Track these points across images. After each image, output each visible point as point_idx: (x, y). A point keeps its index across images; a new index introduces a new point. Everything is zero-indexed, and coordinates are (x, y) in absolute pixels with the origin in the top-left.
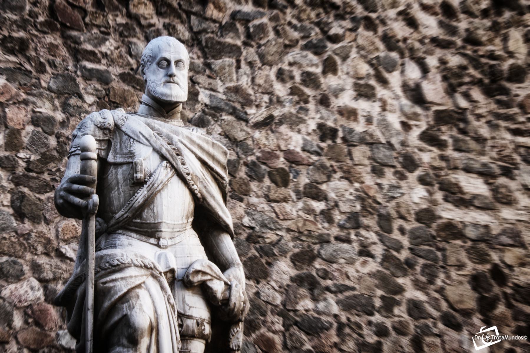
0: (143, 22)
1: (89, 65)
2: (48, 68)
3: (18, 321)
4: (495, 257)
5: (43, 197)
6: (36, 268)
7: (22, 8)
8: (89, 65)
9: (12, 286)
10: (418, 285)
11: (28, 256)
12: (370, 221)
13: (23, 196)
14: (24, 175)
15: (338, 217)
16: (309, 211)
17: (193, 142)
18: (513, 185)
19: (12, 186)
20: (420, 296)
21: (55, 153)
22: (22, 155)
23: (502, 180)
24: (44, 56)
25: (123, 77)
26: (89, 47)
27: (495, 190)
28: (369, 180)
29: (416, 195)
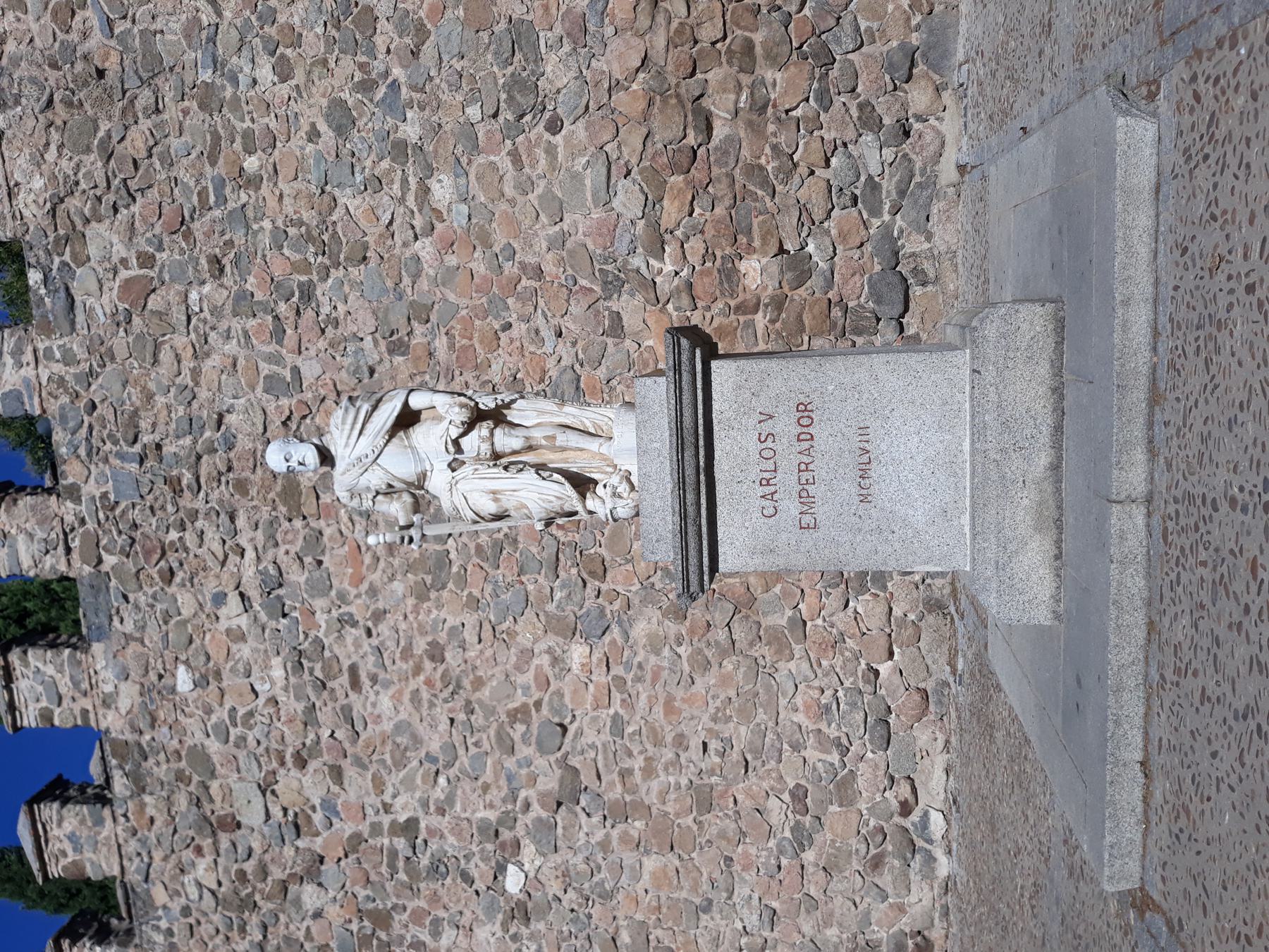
0: (151, 143)
1: (212, 199)
2: (227, 237)
3: (452, 260)
5: (344, 241)
6: (405, 245)
7: (179, 262)
8: (212, 199)
9: (425, 266)
11: (397, 251)
13: (346, 259)
14: (330, 258)
21: (303, 229)
22: (312, 261)
24: (217, 240)
25: (213, 163)
26: (195, 199)
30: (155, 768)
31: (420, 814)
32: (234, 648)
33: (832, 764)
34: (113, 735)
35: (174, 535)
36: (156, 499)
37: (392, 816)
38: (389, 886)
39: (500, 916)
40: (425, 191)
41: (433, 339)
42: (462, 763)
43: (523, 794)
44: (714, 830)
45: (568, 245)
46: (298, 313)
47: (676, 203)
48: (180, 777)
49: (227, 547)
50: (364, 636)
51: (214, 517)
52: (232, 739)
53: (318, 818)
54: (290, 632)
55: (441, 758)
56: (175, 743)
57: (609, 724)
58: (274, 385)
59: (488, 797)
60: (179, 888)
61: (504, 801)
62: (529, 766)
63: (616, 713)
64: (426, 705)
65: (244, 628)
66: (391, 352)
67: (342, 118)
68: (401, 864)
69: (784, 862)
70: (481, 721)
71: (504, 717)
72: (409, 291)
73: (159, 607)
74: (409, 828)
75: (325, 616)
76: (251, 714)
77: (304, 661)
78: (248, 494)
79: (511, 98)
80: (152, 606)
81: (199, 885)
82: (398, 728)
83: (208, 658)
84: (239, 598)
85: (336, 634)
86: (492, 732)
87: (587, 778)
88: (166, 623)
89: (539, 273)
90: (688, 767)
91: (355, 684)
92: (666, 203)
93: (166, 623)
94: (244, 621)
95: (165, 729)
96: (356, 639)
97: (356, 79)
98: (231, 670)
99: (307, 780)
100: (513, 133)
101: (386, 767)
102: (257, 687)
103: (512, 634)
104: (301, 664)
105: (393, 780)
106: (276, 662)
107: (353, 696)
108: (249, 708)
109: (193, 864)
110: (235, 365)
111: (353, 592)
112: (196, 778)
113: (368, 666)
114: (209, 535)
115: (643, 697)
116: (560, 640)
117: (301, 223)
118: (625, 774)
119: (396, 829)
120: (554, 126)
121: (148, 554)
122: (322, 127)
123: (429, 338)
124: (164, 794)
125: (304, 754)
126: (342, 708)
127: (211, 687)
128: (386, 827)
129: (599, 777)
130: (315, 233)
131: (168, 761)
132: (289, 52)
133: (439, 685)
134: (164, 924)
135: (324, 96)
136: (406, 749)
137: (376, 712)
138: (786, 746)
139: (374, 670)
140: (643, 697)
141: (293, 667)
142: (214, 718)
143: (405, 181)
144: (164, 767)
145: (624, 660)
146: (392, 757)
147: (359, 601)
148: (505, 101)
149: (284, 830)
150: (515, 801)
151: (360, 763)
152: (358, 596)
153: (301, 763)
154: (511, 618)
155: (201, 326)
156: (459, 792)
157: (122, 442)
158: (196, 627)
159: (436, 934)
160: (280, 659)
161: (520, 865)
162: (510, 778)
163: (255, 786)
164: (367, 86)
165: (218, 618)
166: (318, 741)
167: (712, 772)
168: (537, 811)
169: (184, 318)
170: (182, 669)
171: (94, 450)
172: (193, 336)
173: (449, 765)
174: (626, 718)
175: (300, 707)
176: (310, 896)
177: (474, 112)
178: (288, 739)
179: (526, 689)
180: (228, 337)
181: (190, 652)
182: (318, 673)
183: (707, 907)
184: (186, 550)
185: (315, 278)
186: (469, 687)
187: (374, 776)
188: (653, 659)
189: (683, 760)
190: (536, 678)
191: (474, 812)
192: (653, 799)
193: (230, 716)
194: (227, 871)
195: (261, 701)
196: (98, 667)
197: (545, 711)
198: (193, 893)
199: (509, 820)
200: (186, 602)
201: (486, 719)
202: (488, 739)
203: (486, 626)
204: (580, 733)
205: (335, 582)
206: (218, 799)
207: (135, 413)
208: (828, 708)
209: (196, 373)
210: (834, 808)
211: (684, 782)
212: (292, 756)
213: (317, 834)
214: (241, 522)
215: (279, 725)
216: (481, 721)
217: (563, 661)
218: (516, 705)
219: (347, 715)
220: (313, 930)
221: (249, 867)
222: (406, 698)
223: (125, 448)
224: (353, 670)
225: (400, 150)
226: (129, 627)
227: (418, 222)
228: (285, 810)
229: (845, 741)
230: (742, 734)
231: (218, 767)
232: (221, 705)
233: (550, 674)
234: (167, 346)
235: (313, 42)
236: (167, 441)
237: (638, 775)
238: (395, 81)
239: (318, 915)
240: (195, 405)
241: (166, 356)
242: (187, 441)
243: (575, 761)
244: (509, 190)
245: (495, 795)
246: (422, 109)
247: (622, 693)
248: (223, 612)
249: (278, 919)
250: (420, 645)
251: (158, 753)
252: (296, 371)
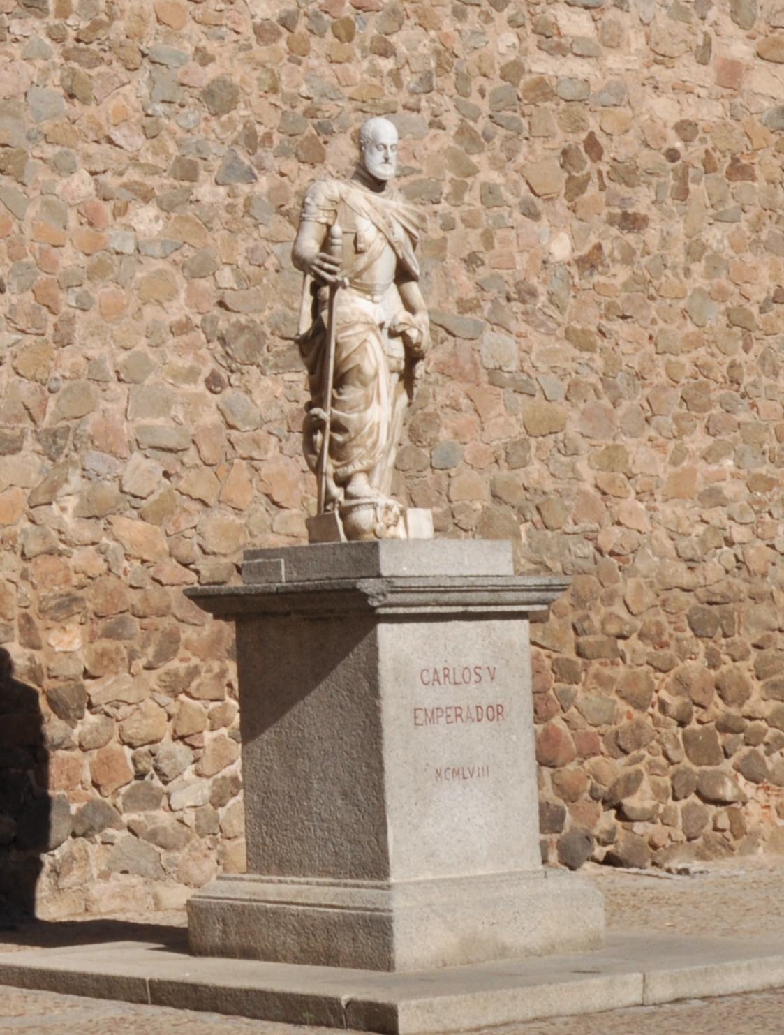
3: (73, 221)
4: (593, 124)
9: (65, 181)
10: (495, 164)
12: (447, 83)
13: (74, 74)
14: (75, 48)
15: (408, 79)
16: (374, 72)
18: (626, 20)
19: (63, 61)
20: (495, 177)
22: (70, 21)
23: (612, 14)
27: (601, 31)
28: (448, 26)
29: (504, 42)
40: (146, 196)
45: (93, 386)
47: (140, 539)
67: (219, 98)
72: (37, 153)
79: (242, 328)
89: (63, 341)
92: (140, 524)
97: (258, 127)
100: (208, 328)
117: (112, 17)
120: (214, 383)
122: (212, 72)
130: (101, 34)
132: (282, 44)
135: (243, 81)
143: (155, 171)
148: (238, 321)
164: (251, 141)
177: (226, 277)
185: (52, 20)
225: (188, 172)
227: (110, 180)
235: (293, 80)
238: (256, 178)
244: (150, 312)
246: (230, 208)
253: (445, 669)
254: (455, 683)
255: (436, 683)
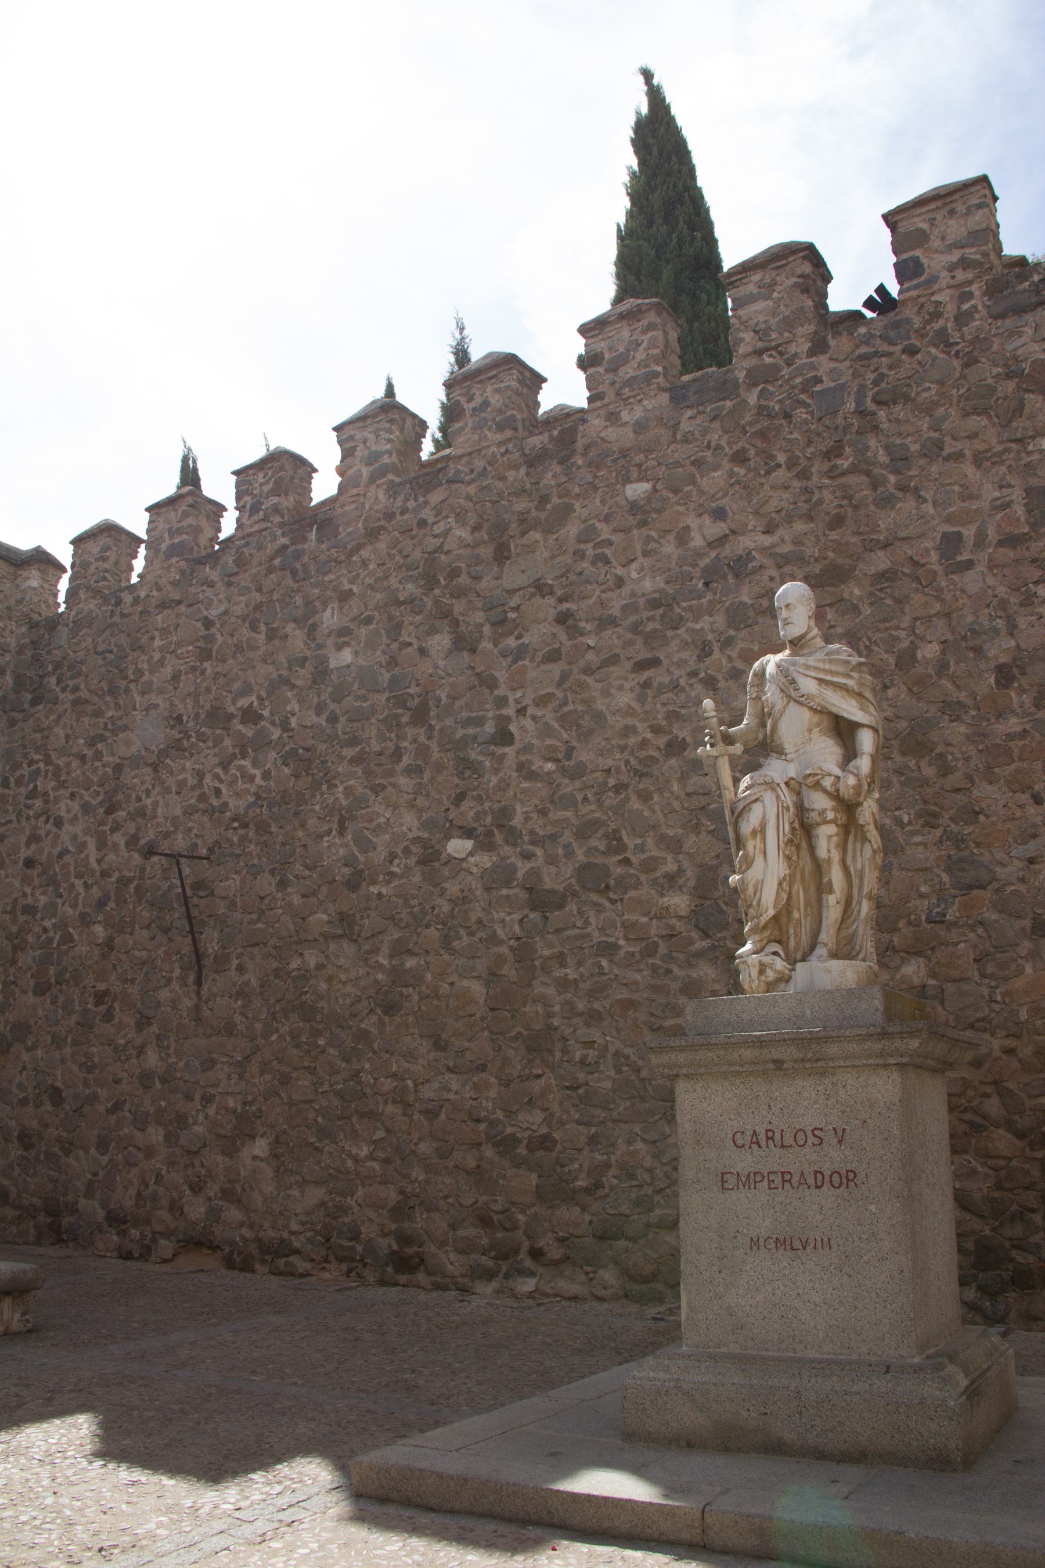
17: (807, 667)
30: (550, 474)
31: (517, 745)
32: (671, 537)
33: (576, 1178)
34: (581, 428)
35: (781, 458)
36: (819, 435)
37: (514, 719)
38: (448, 721)
39: (426, 835)
41: (1017, 715)
42: (567, 785)
43: (539, 852)
44: (510, 1053)
46: (1034, 561)
48: (544, 500)
49: (774, 515)
50: (688, 670)
51: (803, 498)
52: (582, 546)
53: (511, 642)
54: (690, 592)
55: (571, 763)
56: (577, 490)
57: (610, 940)
58: (951, 543)
59: (534, 815)
60: (444, 514)
61: (532, 832)
62: (565, 856)
63: (617, 947)
64: (622, 742)
65: (692, 544)
66: (1000, 669)
68: (470, 731)
69: (483, 1126)
70: (608, 802)
71: (613, 826)
73: (708, 453)
74: (504, 737)
75: (707, 627)
76: (607, 561)
77: (661, 611)
78: (831, 529)
80: (708, 447)
81: (447, 532)
82: (599, 717)
83: (659, 511)
84: (721, 535)
85: (690, 640)
86: (597, 815)
87: (555, 916)
88: (693, 463)
90: (570, 1026)
91: (641, 666)
93: (693, 463)
94: (697, 541)
95: (589, 478)
96: (686, 662)
98: (648, 536)
99: (546, 629)
101: (561, 706)
102: (634, 566)
103: (697, 829)
104: (658, 607)
105: (548, 714)
106: (660, 582)
107: (628, 665)
108: (613, 560)
109: (464, 524)
110: (971, 497)
111: (734, 654)
112: (542, 515)
113: (659, 677)
114: (786, 495)
115: (638, 977)
116: (691, 883)
118: (561, 959)
119: (503, 722)
121: (762, 434)
123: (1019, 710)
124: (528, 486)
125: (570, 622)
126: (617, 655)
127: (631, 518)
128: (504, 712)
129: (558, 931)
131: (559, 485)
133: (643, 754)
134: (411, 504)
136: (579, 726)
137: (612, 691)
138: (593, 1130)
139: (655, 684)
140: (638, 977)
141: (655, 599)
142: (600, 526)
144: (553, 483)
145: (674, 954)
146: (570, 712)
147: (724, 661)
149: (500, 609)
150: (532, 843)
151: (564, 677)
152: (730, 659)
153: (562, 619)
154: (713, 827)
155: (1012, 456)
156: (539, 785)
157: (876, 389)
158: (688, 495)
159: (409, 771)
160: (662, 585)
161: (471, 854)
162: (554, 837)
163: (539, 575)
165: (700, 515)
166: (582, 634)
167: (565, 1051)
168: (523, 868)
169: (1019, 435)
170: (646, 486)
171: (866, 362)
172: (999, 448)
173: (564, 771)
174: (616, 959)
175: (616, 611)
176: (441, 641)
178: (584, 604)
179: (641, 848)
180: (1001, 487)
181: (665, 493)
182: (650, 626)
183: (440, 1045)
184: (768, 473)
186: (641, 786)
187: (553, 694)
188: (676, 986)
189: (576, 1020)
190: (652, 858)
191: (521, 801)
192: (538, 989)
193: (603, 541)
194: (459, 558)
195: (620, 571)
196: (646, 402)
197: (619, 870)
198: (438, 529)
199: (513, 837)
200: (715, 480)
201: (610, 808)
202: (590, 810)
203: (703, 801)
204: (598, 908)
205: (743, 634)
206: (524, 541)
207: (907, 398)
208: (631, 1176)
209: (959, 456)
210: (534, 1179)
211: (556, 1021)
212: (568, 610)
213: (495, 645)
214: (800, 526)
215: (597, 593)
216: (608, 802)
217: (671, 887)
218: (625, 838)
219: (613, 660)
220: (409, 649)
221: (463, 580)
222: (630, 721)
223: (870, 394)
224: (655, 662)
226: (685, 426)
228: (517, 609)
229: (600, 1193)
230: (605, 1082)
231: (555, 537)
232: (615, 531)
233: (658, 874)
234: (985, 421)
236: (881, 437)
237: (558, 973)
239: (423, 652)
240: (922, 462)
241: (977, 422)
242: (883, 458)
243: (572, 907)
245: (537, 824)
247: (640, 952)
248: (707, 520)
249: (418, 614)
250: (683, 733)
251: (566, 475)
252: (969, 565)
253: (767, 1131)
254: (782, 1146)
255: (755, 1147)
